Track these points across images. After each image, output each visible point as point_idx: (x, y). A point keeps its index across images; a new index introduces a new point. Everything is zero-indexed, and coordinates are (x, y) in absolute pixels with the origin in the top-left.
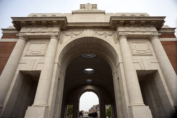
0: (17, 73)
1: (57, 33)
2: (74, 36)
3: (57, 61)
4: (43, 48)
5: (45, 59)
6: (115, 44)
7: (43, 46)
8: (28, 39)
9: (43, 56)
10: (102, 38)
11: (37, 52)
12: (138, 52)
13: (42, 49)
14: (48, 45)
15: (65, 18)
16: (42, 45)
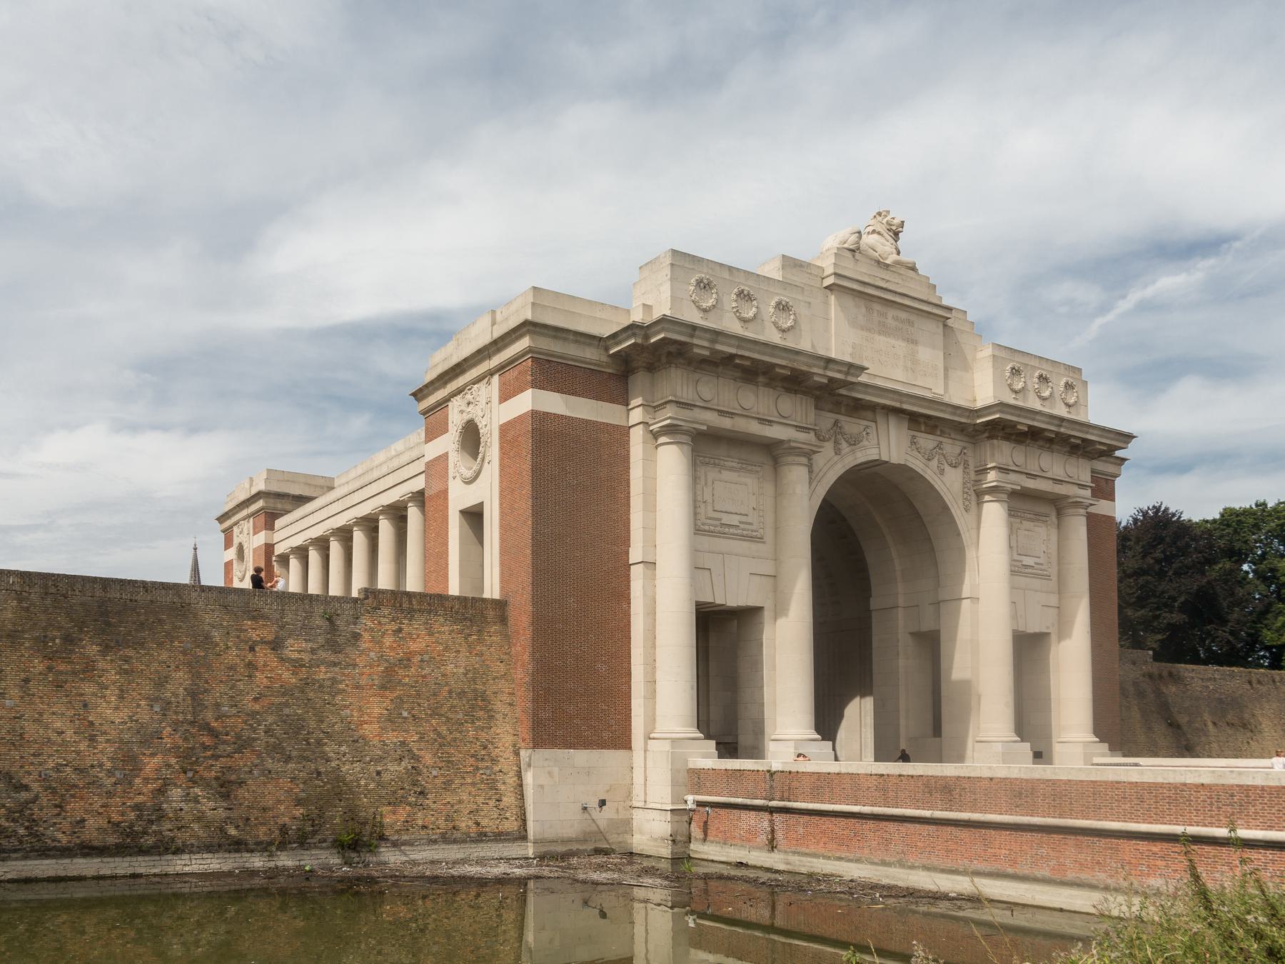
10: (929, 472)
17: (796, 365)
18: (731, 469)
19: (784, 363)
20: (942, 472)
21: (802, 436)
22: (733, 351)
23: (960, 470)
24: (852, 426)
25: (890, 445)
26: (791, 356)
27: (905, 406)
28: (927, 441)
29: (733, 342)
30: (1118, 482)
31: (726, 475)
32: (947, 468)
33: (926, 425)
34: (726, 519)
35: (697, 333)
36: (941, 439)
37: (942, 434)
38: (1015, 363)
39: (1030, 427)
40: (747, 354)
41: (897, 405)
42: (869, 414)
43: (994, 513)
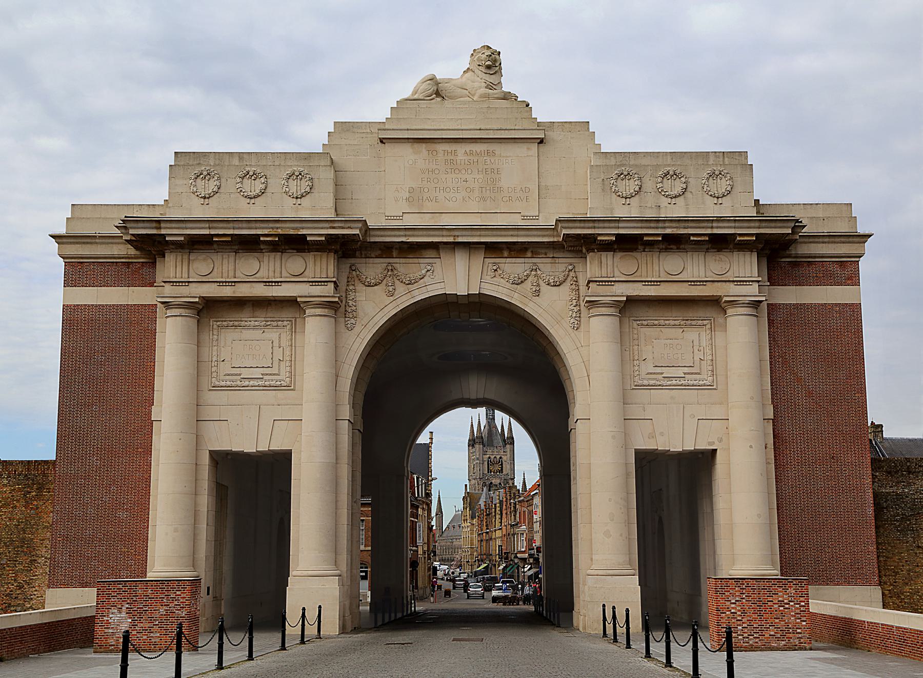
0: (206, 460)
1: (332, 285)
2: (401, 289)
3: (346, 412)
4: (278, 354)
5: (290, 394)
6: (571, 330)
7: (276, 344)
8: (207, 310)
9: (288, 388)
10: (516, 298)
11: (257, 373)
12: (659, 370)
13: (276, 359)
14: (293, 331)
15: (360, 225)
16: (273, 334)
17: (280, 231)
18: (255, 327)
19: (266, 232)
20: (537, 293)
21: (317, 290)
22: (206, 232)
23: (566, 288)
24: (406, 267)
25: (456, 278)
26: (271, 225)
27: (460, 240)
28: (515, 267)
29: (203, 225)
30: (864, 265)
31: (247, 334)
32: (544, 288)
33: (510, 250)
34: (246, 373)
35: (162, 225)
36: (534, 260)
37: (535, 254)
38: (624, 168)
39: (617, 235)
40: (221, 232)
41: (451, 240)
42: (432, 253)
43: (601, 326)
